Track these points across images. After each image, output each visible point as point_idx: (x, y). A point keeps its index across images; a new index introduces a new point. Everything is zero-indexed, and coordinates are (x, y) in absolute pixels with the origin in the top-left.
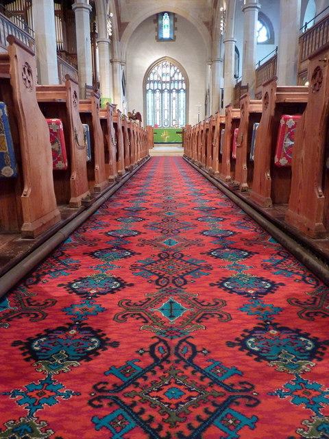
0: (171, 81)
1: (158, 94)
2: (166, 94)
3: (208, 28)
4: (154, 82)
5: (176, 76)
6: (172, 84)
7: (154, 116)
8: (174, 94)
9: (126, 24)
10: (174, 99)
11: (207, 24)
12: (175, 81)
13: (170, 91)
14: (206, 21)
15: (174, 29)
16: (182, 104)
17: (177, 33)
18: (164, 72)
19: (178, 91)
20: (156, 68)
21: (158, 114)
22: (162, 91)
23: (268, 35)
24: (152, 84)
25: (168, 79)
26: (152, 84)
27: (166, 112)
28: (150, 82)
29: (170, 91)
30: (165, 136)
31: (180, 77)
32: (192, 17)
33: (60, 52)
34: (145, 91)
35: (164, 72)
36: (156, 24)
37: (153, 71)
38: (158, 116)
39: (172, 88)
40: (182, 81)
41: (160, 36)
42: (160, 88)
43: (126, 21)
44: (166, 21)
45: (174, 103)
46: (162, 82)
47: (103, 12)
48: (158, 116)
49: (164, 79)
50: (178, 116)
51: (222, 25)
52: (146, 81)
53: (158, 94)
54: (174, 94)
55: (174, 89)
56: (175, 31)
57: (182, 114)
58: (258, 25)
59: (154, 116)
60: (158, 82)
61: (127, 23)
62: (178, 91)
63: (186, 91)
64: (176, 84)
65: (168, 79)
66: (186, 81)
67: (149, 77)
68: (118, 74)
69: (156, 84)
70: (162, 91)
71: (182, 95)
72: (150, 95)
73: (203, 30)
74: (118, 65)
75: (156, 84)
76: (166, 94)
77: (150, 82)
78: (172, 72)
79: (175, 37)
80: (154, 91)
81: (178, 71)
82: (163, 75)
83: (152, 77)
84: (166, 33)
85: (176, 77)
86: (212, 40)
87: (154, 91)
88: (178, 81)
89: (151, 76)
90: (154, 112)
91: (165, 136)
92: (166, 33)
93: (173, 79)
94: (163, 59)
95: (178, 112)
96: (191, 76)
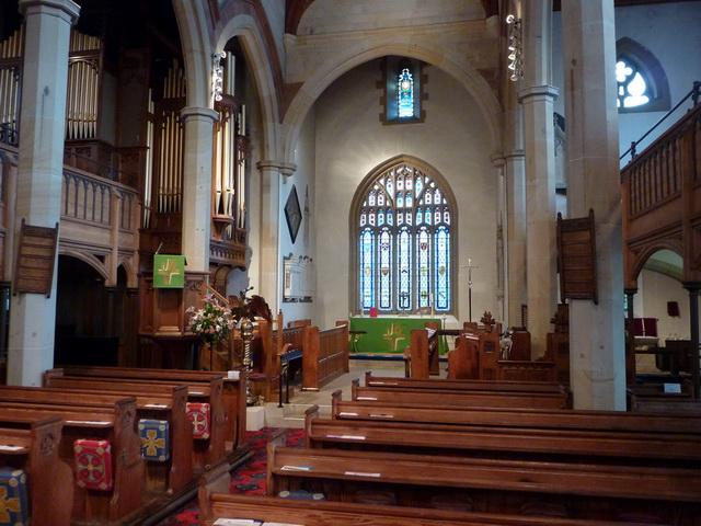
0: (414, 211)
4: (376, 210)
6: (419, 214)
7: (376, 287)
8: (424, 237)
10: (424, 246)
11: (486, 73)
14: (484, 67)
15: (421, 97)
16: (443, 259)
17: (427, 106)
18: (400, 188)
19: (433, 230)
20: (382, 181)
21: (385, 279)
22: (395, 231)
25: (409, 204)
27: (404, 276)
28: (369, 210)
30: (394, 337)
31: (438, 200)
32: (449, 60)
33: (75, 147)
34: (356, 232)
35: (402, 188)
36: (382, 90)
37: (376, 187)
38: (385, 290)
39: (418, 223)
40: (442, 208)
43: (295, 80)
45: (424, 255)
46: (396, 211)
47: (196, 45)
48: (385, 290)
49: (400, 205)
50: (433, 286)
51: (512, 57)
52: (358, 206)
54: (424, 237)
55: (423, 224)
56: (424, 102)
57: (443, 281)
58: (622, 70)
59: (376, 287)
60: (386, 210)
61: (299, 85)
62: (433, 230)
63: (452, 230)
64: (428, 214)
65: (409, 204)
66: (451, 207)
67: (366, 199)
68: (273, 194)
70: (395, 231)
71: (443, 238)
72: (367, 238)
73: (480, 89)
74: (273, 175)
77: (369, 210)
78: (419, 187)
79: (423, 113)
80: (377, 231)
81: (432, 185)
82: (397, 194)
83: (372, 201)
84: (406, 109)
85: (428, 199)
86: (504, 111)
87: (377, 231)
88: (433, 208)
90: (376, 277)
91: (394, 337)
92: (406, 109)
93: (421, 203)
94: (397, 161)
95: (432, 276)
96: (456, 192)
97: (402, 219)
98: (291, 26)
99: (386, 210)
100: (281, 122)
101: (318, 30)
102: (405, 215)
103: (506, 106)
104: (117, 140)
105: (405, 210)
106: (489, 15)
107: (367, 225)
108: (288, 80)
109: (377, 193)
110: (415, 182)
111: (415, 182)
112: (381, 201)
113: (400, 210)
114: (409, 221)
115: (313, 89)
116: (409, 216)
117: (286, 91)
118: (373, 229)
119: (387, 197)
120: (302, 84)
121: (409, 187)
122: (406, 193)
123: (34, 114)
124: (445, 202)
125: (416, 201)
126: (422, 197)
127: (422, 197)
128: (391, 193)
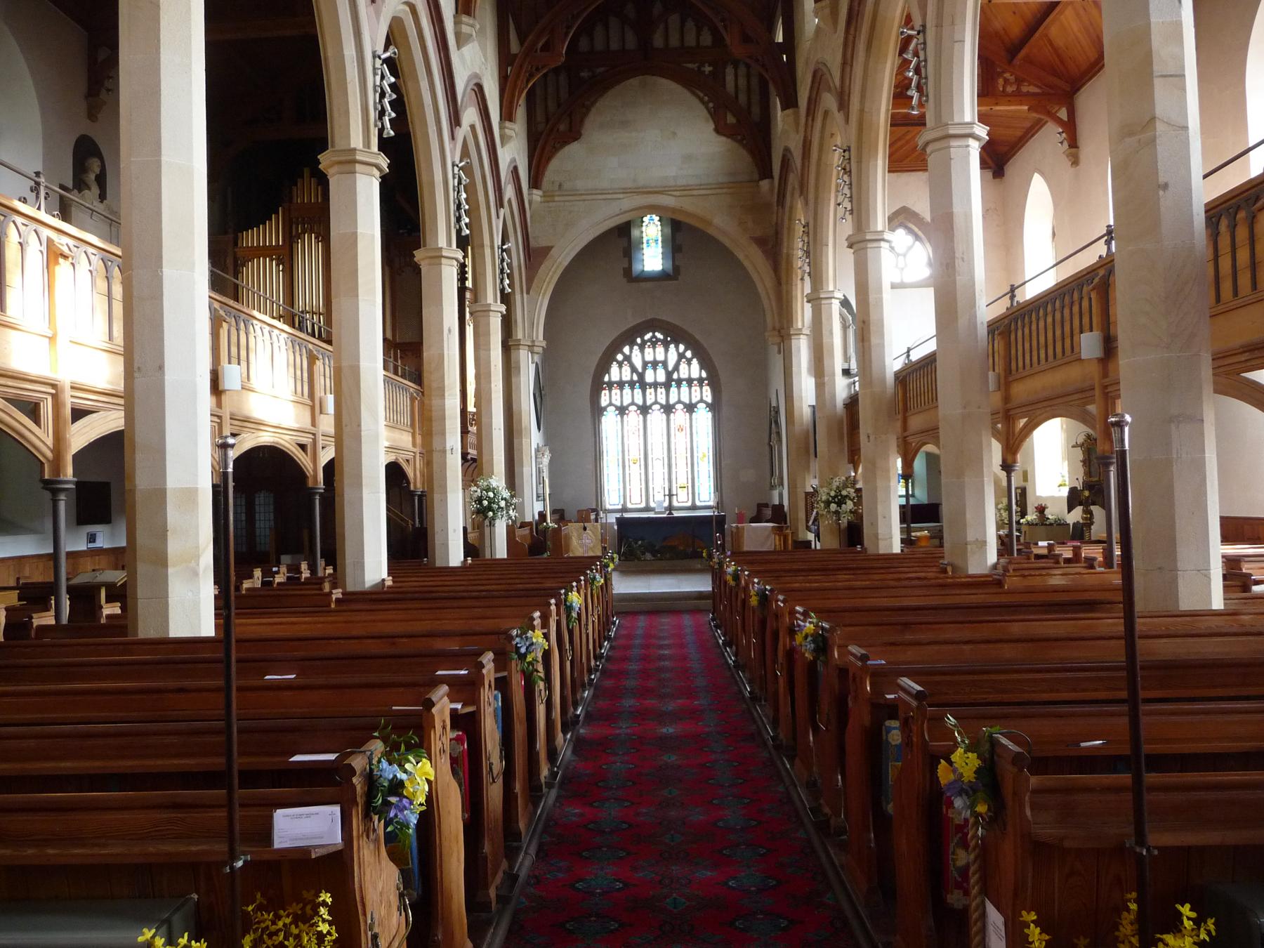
1: (634, 417)
2: (656, 417)
3: (765, 252)
4: (621, 384)
5: (684, 372)
6: (674, 390)
8: (680, 416)
9: (546, 251)
11: (761, 242)
12: (679, 382)
13: (668, 409)
18: (649, 357)
19: (690, 408)
20: (626, 350)
22: (644, 410)
23: (930, 264)
24: (616, 392)
26: (616, 392)
28: (610, 385)
29: (668, 409)
31: (695, 370)
37: (620, 357)
41: (637, 268)
42: (639, 401)
44: (652, 231)
45: (680, 441)
53: (634, 417)
54: (680, 416)
55: (679, 402)
60: (632, 384)
61: (549, 249)
62: (690, 408)
65: (661, 377)
67: (608, 371)
69: (627, 390)
75: (627, 390)
76: (656, 417)
77: (610, 385)
79: (676, 269)
80: (622, 410)
82: (645, 364)
83: (615, 373)
84: (652, 259)
85: (684, 372)
87: (622, 410)
88: (690, 381)
89: (614, 368)
92: (652, 259)
93: (675, 376)
97: (653, 396)
98: (535, 182)
99: (632, 384)
100: (528, 293)
101: (567, 186)
102: (656, 391)
103: (784, 280)
104: (394, 335)
105: (655, 385)
106: (762, 179)
107: (611, 404)
108: (533, 244)
109: (620, 365)
110: (667, 350)
111: (667, 350)
112: (627, 374)
113: (651, 385)
114: (662, 399)
115: (563, 255)
116: (661, 391)
117: (535, 256)
118: (617, 408)
119: (634, 369)
120: (552, 247)
121: (660, 356)
122: (655, 364)
123: (443, 350)
124: (704, 375)
125: (669, 375)
126: (676, 368)
127: (676, 368)
128: (639, 366)
